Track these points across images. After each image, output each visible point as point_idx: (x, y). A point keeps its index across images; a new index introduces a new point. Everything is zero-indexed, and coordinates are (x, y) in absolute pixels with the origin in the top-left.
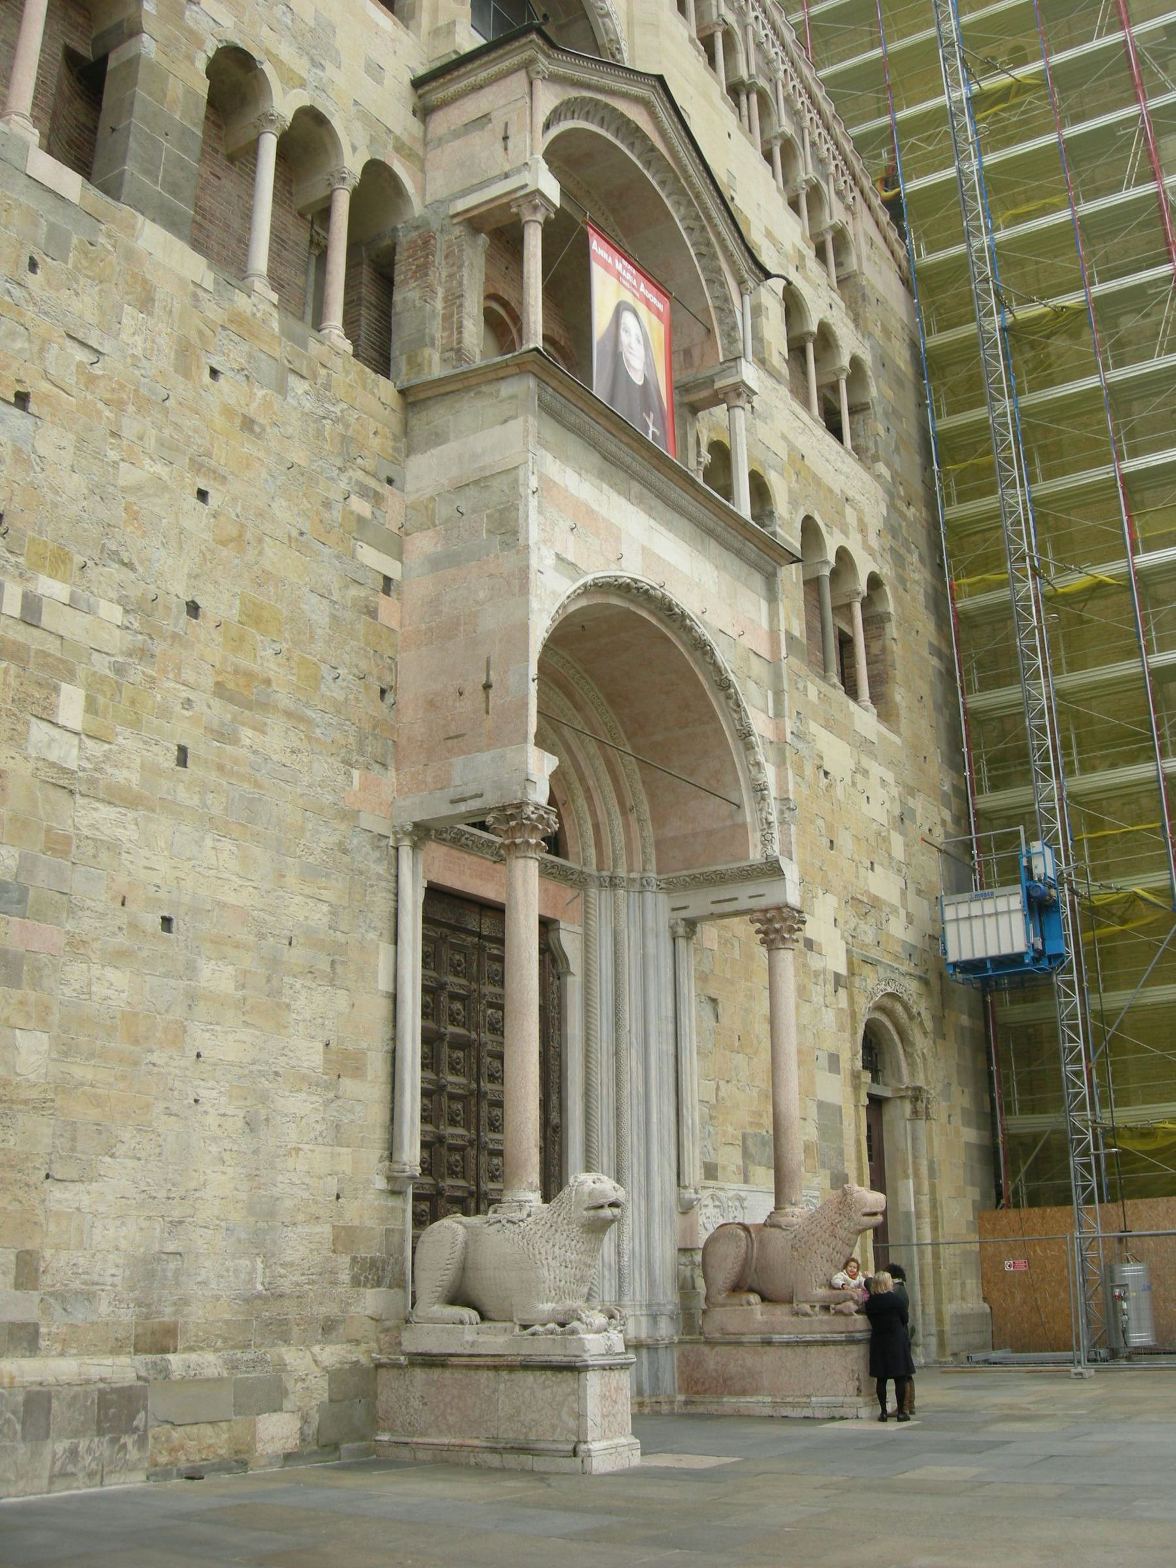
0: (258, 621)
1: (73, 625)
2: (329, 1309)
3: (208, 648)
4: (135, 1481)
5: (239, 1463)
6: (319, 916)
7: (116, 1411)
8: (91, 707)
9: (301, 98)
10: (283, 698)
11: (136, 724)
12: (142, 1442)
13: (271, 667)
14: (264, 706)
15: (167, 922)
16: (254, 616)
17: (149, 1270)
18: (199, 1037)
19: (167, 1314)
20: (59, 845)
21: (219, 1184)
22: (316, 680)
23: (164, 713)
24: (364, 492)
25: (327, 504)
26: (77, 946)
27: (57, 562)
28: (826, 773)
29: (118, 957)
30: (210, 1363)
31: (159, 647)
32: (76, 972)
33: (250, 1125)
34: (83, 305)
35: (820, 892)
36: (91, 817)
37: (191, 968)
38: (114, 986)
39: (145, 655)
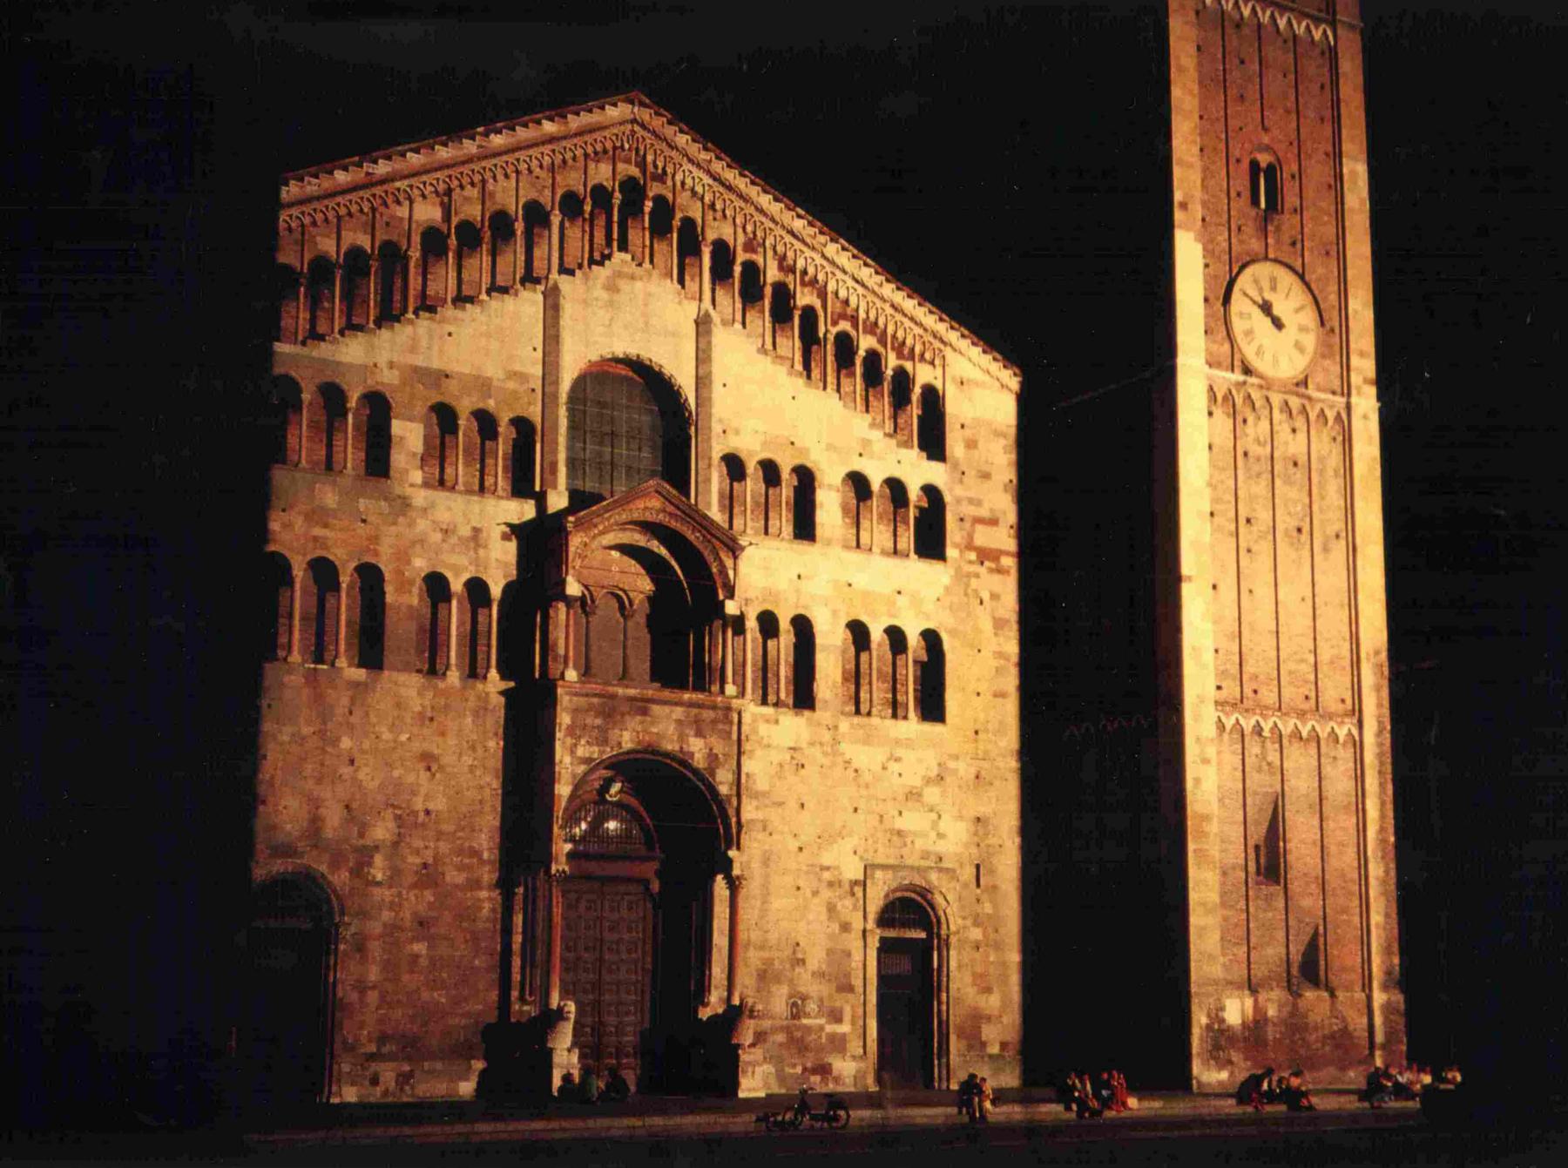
9: (466, 576)
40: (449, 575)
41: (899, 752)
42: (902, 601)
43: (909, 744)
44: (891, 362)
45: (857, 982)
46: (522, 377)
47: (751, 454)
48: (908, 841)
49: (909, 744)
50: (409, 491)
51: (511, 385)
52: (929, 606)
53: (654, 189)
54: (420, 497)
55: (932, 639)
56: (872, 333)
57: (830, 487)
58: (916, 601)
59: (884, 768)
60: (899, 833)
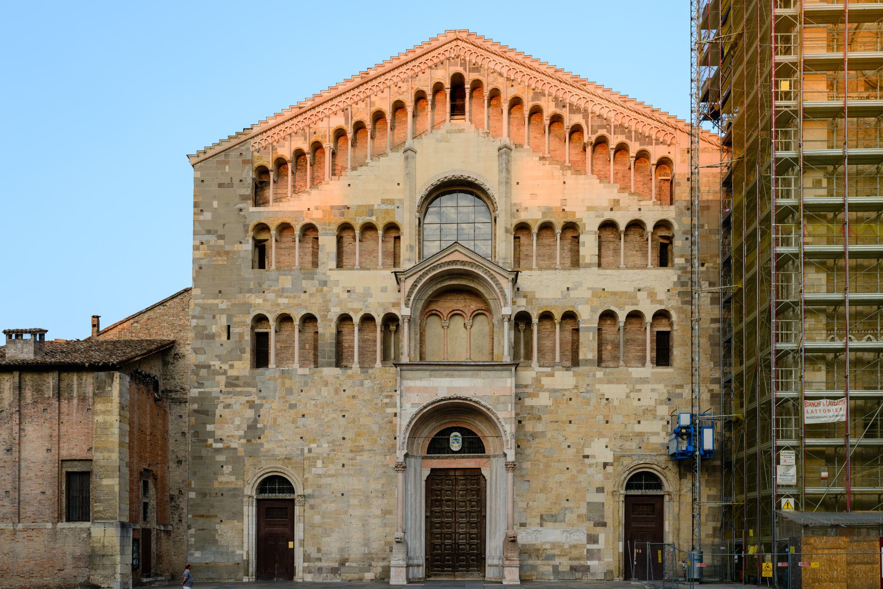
0: (359, 435)
1: (318, 450)
2: (385, 556)
3: (348, 444)
4: (339, 581)
5: (361, 579)
6: (379, 486)
7: (334, 571)
8: (323, 463)
9: (361, 313)
10: (367, 448)
11: (333, 463)
12: (340, 575)
13: (363, 443)
14: (362, 451)
15: (343, 494)
16: (358, 435)
17: (342, 550)
18: (351, 512)
19: (346, 556)
20: (319, 486)
21: (357, 536)
22: (376, 441)
23: (339, 459)
24: (387, 397)
25: (376, 404)
26: (324, 501)
27: (314, 441)
28: (607, 399)
29: (333, 501)
30: (354, 565)
31: (336, 448)
32: (324, 506)
33: (363, 525)
34: (313, 392)
35: (596, 439)
36: (324, 481)
37: (348, 501)
38: (332, 507)
39: (334, 450)
40: (351, 314)
41: (638, 387)
42: (642, 296)
43: (644, 381)
44: (634, 148)
45: (609, 520)
46: (391, 202)
47: (537, 220)
48: (645, 440)
49: (644, 381)
50: (328, 273)
51: (384, 207)
52: (662, 295)
53: (469, 78)
54: (337, 275)
55: (662, 315)
56: (623, 133)
57: (589, 232)
58: (652, 295)
59: (628, 397)
60: (640, 435)
